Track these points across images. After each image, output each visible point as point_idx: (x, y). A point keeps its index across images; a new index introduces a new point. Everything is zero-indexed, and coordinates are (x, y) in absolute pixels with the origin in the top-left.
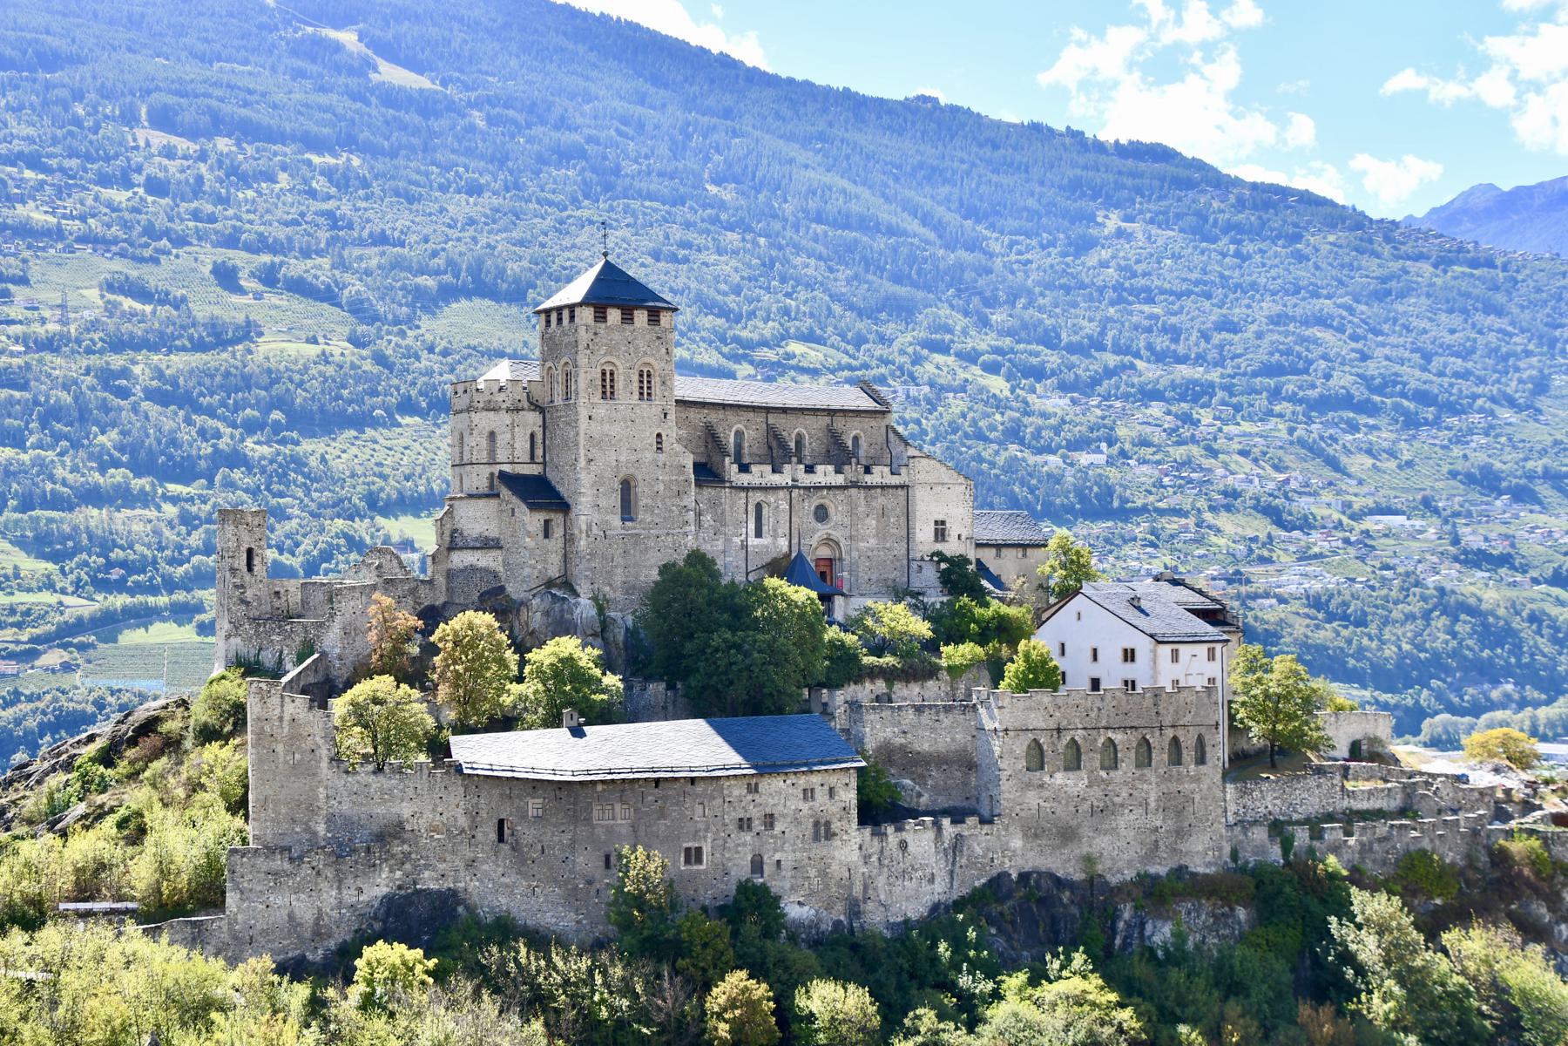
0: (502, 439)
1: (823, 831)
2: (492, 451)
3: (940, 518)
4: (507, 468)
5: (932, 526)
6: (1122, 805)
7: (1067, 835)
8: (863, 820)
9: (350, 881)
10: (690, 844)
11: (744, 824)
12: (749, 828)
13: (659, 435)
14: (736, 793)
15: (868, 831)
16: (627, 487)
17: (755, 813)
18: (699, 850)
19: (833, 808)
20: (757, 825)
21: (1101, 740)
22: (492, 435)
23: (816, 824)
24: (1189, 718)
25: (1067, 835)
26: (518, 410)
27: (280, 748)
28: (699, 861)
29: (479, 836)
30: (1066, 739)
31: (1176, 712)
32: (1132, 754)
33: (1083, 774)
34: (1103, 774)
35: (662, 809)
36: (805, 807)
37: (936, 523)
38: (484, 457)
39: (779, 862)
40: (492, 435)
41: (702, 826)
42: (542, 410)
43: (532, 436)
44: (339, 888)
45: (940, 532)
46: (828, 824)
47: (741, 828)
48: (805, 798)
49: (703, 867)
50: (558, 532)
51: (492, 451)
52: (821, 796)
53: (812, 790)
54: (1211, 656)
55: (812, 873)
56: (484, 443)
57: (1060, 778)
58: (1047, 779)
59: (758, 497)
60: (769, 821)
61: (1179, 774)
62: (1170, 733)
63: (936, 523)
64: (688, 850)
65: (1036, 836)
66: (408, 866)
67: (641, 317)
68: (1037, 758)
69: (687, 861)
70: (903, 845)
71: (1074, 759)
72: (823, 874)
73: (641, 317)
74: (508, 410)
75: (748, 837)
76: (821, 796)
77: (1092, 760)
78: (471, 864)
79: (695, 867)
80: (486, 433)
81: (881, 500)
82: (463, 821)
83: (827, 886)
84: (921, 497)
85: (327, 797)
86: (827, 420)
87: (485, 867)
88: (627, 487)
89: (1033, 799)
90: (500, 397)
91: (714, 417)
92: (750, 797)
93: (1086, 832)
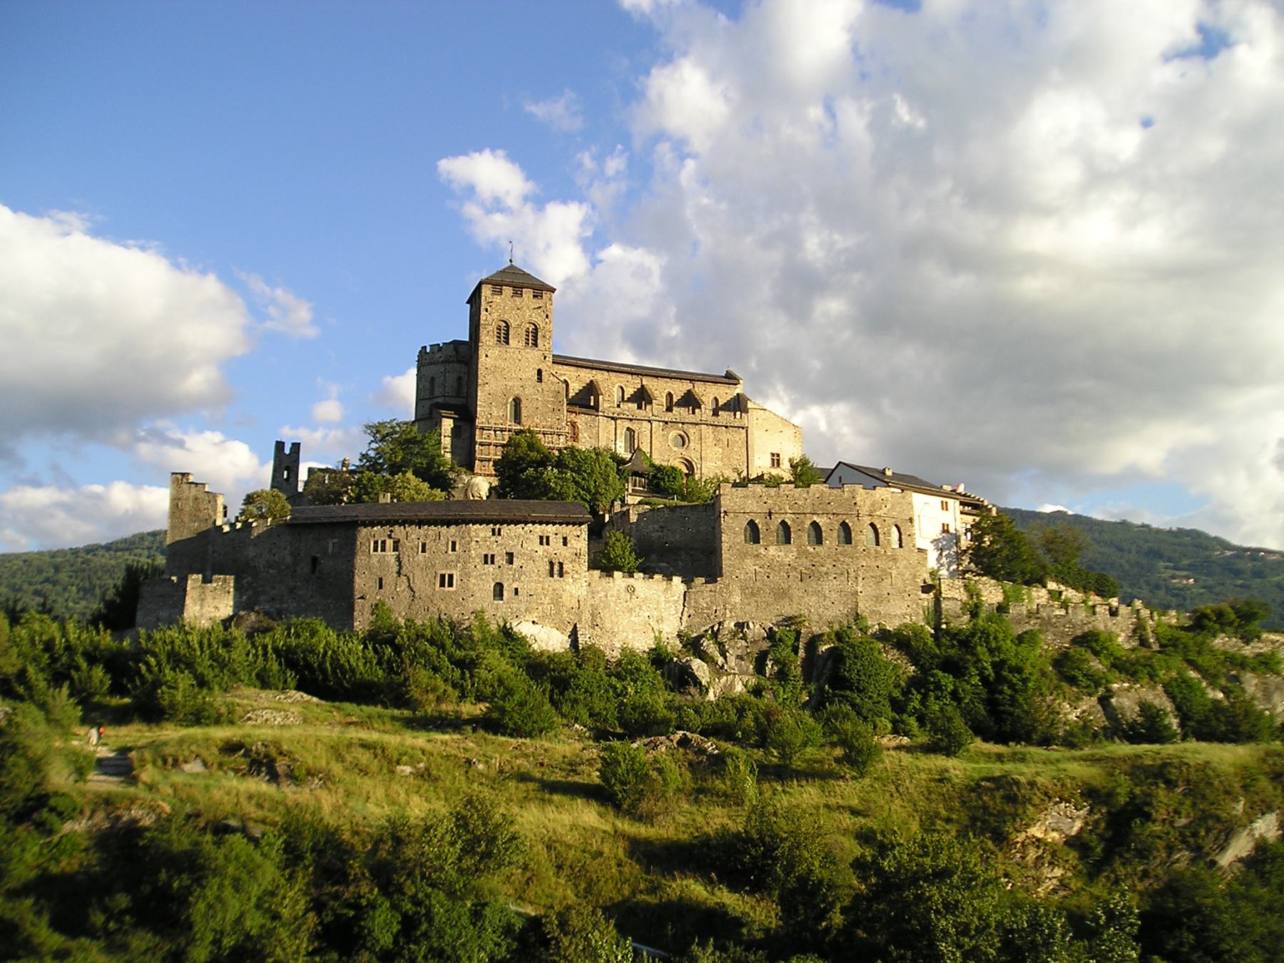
0: (439, 380)
1: (556, 569)
2: (432, 391)
3: (774, 452)
4: (440, 400)
5: (769, 457)
6: (826, 574)
7: (781, 594)
8: (593, 566)
9: (209, 599)
10: (443, 572)
11: (488, 559)
12: (493, 562)
13: (540, 372)
14: (482, 535)
15: (597, 573)
16: (517, 402)
17: (495, 550)
18: (451, 576)
19: (564, 553)
20: (501, 560)
21: (809, 522)
22: (433, 379)
23: (551, 564)
24: (885, 510)
25: (781, 594)
26: (449, 362)
27: (186, 519)
28: (451, 585)
29: (299, 570)
30: (777, 520)
31: (873, 505)
32: (835, 534)
33: (792, 547)
34: (811, 550)
35: (424, 545)
36: (541, 550)
37: (773, 455)
38: (427, 395)
39: (516, 590)
40: (433, 379)
41: (453, 558)
42: (467, 364)
43: (459, 379)
44: (202, 606)
45: (776, 460)
46: (561, 564)
47: (486, 562)
48: (541, 543)
49: (451, 589)
50: (466, 435)
51: (432, 391)
52: (556, 543)
53: (548, 538)
54: (945, 507)
55: (547, 600)
56: (427, 384)
57: (772, 550)
58: (762, 551)
59: (627, 424)
60: (510, 557)
61: (876, 552)
62: (867, 520)
63: (773, 455)
64: (443, 576)
65: (753, 594)
66: (250, 592)
67: (527, 293)
68: (753, 533)
69: (442, 585)
70: (631, 590)
71: (786, 533)
72: (556, 601)
73: (527, 293)
74: (443, 362)
75: (490, 568)
76: (556, 543)
77: (801, 537)
78: (292, 591)
79: (447, 589)
80: (429, 379)
81: (724, 435)
82: (289, 559)
83: (559, 612)
84: (757, 436)
85: (214, 552)
86: (690, 386)
87: (301, 592)
88: (517, 402)
89: (750, 565)
90: (440, 354)
91: (599, 377)
92: (493, 538)
93: (796, 593)
